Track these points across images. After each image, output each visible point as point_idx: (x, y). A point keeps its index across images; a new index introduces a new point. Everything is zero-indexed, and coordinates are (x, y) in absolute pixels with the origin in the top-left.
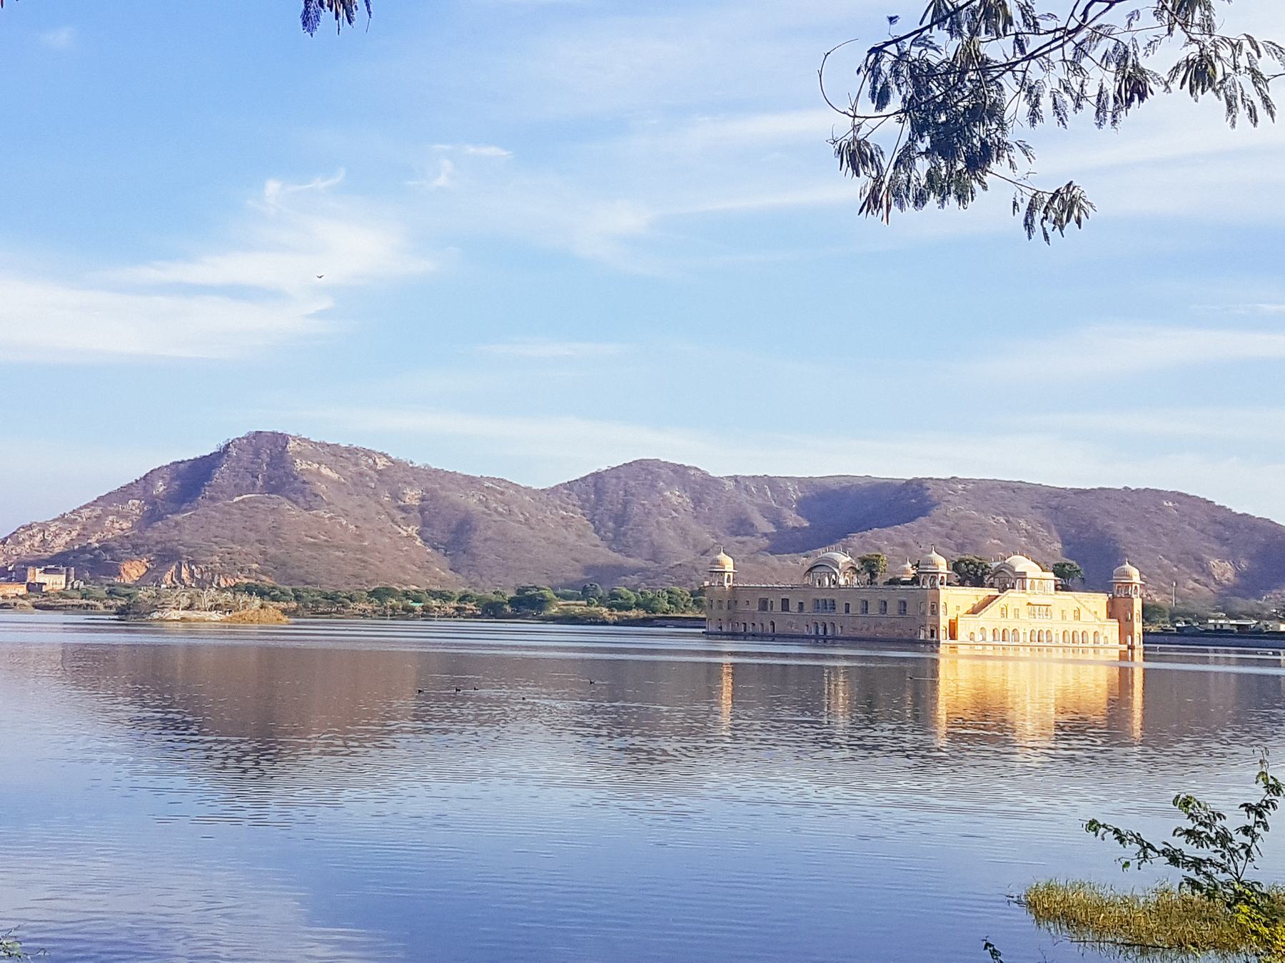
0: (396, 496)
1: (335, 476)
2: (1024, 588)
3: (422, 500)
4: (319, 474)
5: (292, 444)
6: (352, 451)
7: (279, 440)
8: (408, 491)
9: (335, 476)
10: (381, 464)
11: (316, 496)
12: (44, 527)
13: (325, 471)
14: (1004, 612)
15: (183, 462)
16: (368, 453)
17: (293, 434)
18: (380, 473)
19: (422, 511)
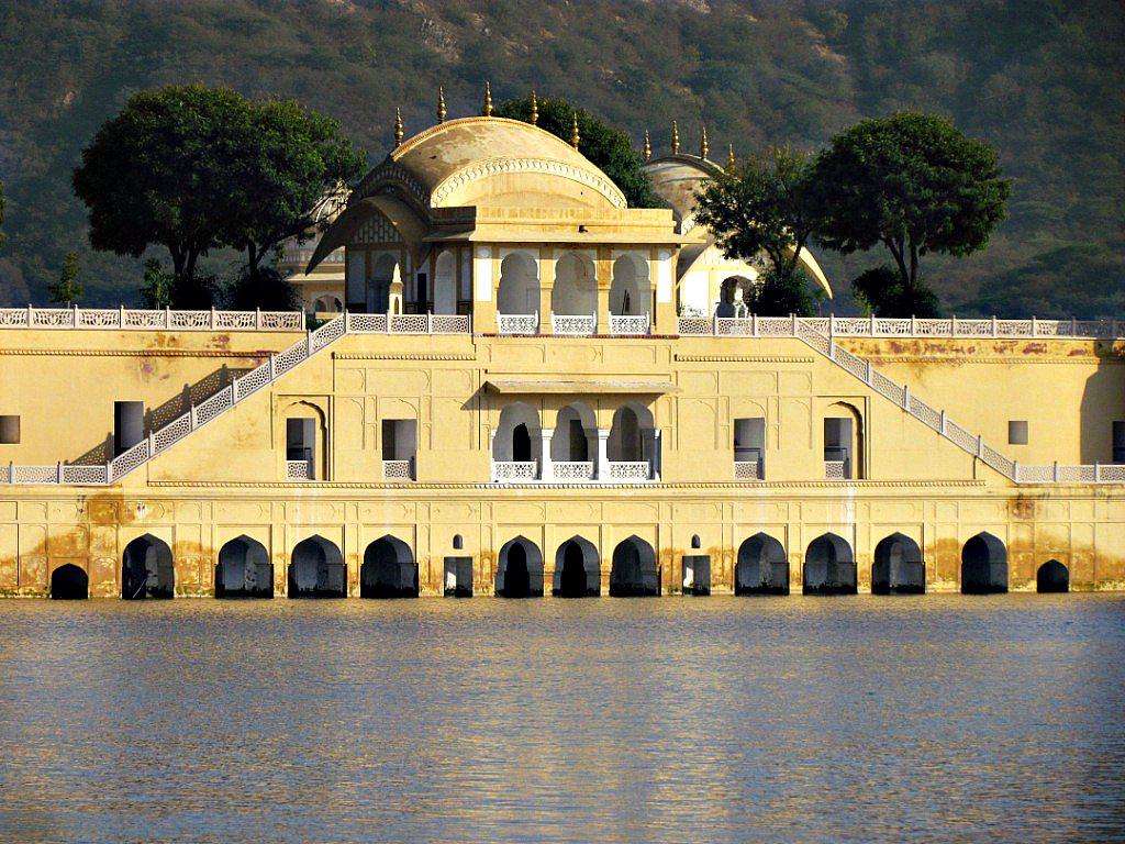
2: (465, 306)
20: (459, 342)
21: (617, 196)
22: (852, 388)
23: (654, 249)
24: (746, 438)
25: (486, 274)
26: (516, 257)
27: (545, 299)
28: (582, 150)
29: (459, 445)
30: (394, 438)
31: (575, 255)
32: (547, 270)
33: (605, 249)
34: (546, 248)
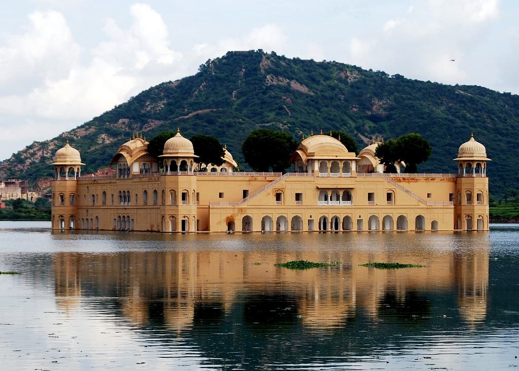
0: (364, 106)
1: (304, 89)
2: (313, 171)
3: (392, 108)
4: (287, 90)
5: (265, 63)
6: (326, 67)
7: (254, 57)
8: (376, 101)
9: (304, 89)
10: (352, 78)
11: (281, 108)
12: (44, 145)
13: (295, 85)
14: (278, 197)
15: (170, 82)
16: (342, 67)
17: (269, 53)
18: (352, 86)
19: (388, 118)
20: (312, 179)
21: (346, 150)
22: (392, 187)
23: (351, 160)
24: (370, 196)
25: (317, 166)
26: (323, 162)
27: (329, 170)
28: (341, 141)
29: (311, 198)
30: (298, 197)
31: (335, 163)
32: (329, 165)
33: (341, 160)
34: (329, 160)
